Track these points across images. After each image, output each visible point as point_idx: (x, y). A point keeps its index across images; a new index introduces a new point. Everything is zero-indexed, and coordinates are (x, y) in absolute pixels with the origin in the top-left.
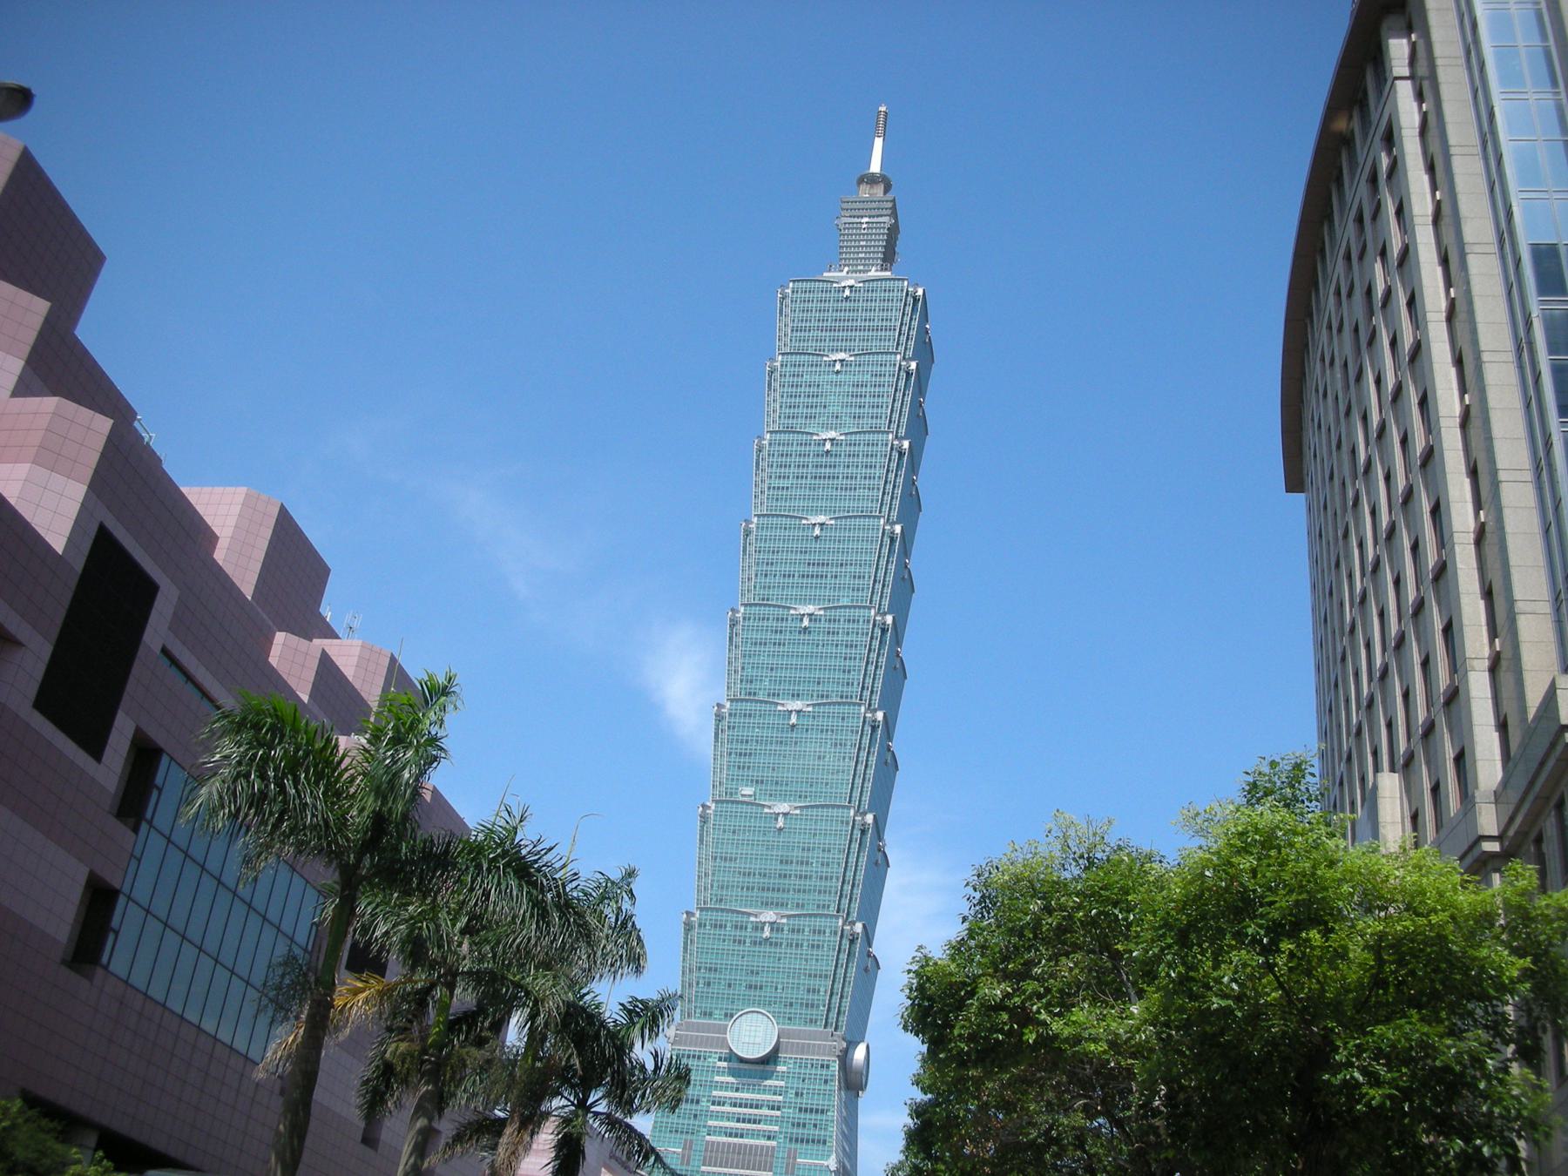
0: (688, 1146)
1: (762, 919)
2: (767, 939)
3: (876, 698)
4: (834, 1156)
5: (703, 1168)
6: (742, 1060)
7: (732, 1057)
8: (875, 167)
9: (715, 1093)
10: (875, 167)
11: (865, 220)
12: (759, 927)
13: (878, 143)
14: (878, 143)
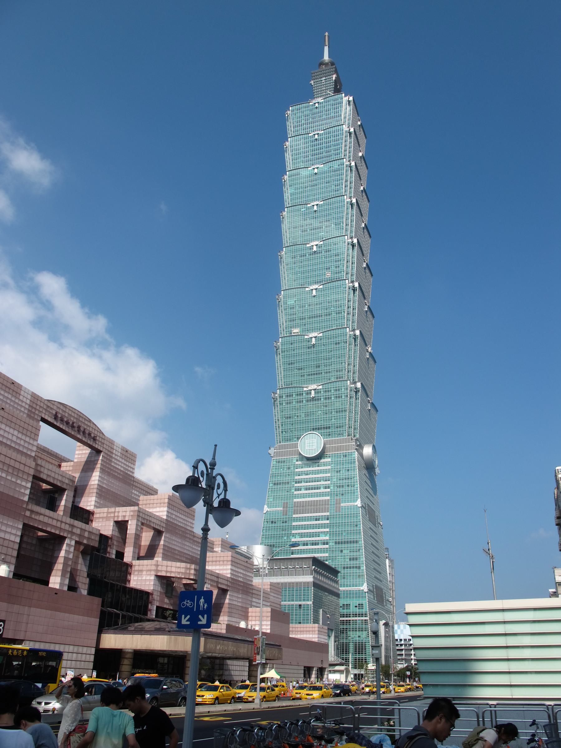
0: (285, 506)
1: (310, 388)
2: (313, 398)
3: (354, 278)
4: (359, 500)
5: (294, 516)
6: (308, 459)
7: (302, 458)
8: (326, 57)
9: (297, 477)
10: (326, 57)
11: (323, 79)
12: (309, 393)
13: (326, 49)
14: (326, 49)
